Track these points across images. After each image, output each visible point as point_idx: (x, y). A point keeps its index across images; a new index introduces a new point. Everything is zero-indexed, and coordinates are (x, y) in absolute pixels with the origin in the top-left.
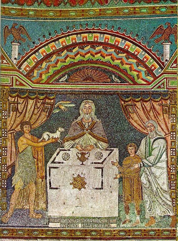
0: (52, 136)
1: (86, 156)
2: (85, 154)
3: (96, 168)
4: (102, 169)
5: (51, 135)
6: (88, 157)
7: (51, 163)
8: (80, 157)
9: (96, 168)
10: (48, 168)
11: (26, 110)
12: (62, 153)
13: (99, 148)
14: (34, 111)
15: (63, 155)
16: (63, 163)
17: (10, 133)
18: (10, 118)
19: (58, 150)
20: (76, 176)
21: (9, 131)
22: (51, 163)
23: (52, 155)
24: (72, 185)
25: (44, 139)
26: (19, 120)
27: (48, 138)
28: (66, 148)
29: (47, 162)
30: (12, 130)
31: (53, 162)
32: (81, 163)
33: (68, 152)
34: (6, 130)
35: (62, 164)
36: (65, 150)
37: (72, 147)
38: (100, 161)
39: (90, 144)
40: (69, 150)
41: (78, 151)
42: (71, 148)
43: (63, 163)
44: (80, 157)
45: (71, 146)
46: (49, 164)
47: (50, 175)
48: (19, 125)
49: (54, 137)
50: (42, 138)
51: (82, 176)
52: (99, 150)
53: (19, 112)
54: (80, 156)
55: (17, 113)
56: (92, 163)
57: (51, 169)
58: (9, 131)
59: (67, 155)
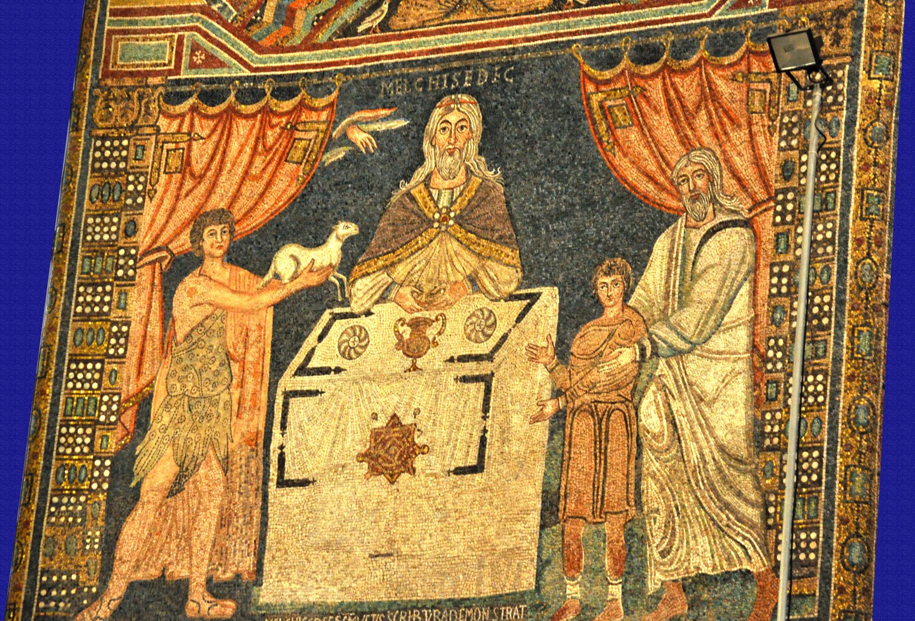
0: (309, 261)
1: (431, 332)
2: (428, 322)
3: (465, 379)
4: (486, 380)
5: (306, 255)
6: (440, 333)
7: (296, 374)
8: (406, 336)
9: (465, 379)
10: (279, 400)
11: (222, 161)
12: (339, 326)
13: (487, 293)
14: (251, 163)
15: (345, 337)
16: (338, 370)
17: (150, 263)
18: (156, 201)
19: (326, 316)
20: (381, 423)
21: (146, 253)
22: (296, 374)
23: (300, 338)
24: (365, 465)
25: (277, 276)
26: (186, 209)
27: (293, 269)
28: (355, 308)
29: (278, 368)
30: (159, 250)
31: (303, 370)
32: (408, 363)
33: (363, 321)
34: (133, 252)
35: (337, 376)
36: (353, 315)
37: (383, 299)
38: (484, 348)
39: (452, 279)
40: (368, 313)
41: (403, 314)
42: (377, 302)
43: (338, 370)
44: (406, 336)
45: (376, 297)
46: (288, 382)
47: (283, 426)
48: (185, 225)
49: (317, 265)
50: (269, 276)
51: (407, 420)
52: (481, 301)
53: (192, 175)
54: (406, 332)
55: (183, 178)
56: (451, 360)
57: (292, 401)
58: (146, 253)
59: (358, 332)
